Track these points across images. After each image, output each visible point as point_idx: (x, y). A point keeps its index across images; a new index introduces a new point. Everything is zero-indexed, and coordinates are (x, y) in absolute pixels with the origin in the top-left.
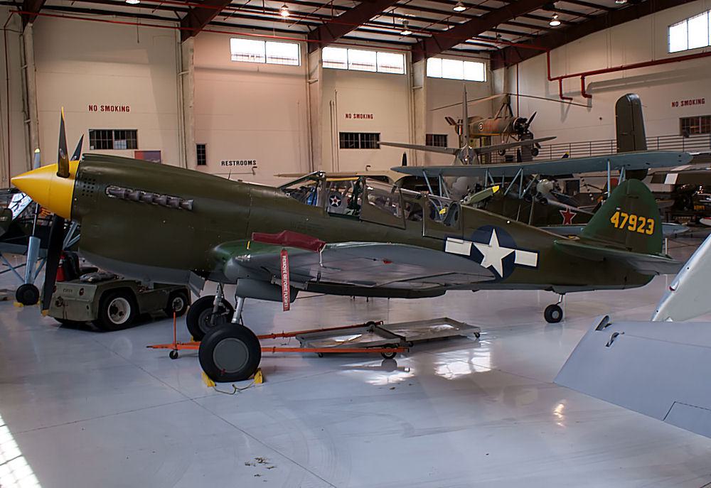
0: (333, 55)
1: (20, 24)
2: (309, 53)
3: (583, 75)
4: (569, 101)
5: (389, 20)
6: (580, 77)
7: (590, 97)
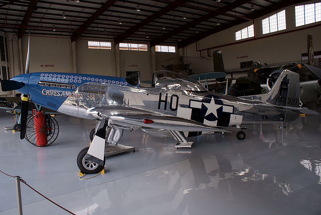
0: (123, 45)
1: (17, 39)
2: (115, 45)
3: (208, 49)
5: (141, 33)
6: (207, 50)
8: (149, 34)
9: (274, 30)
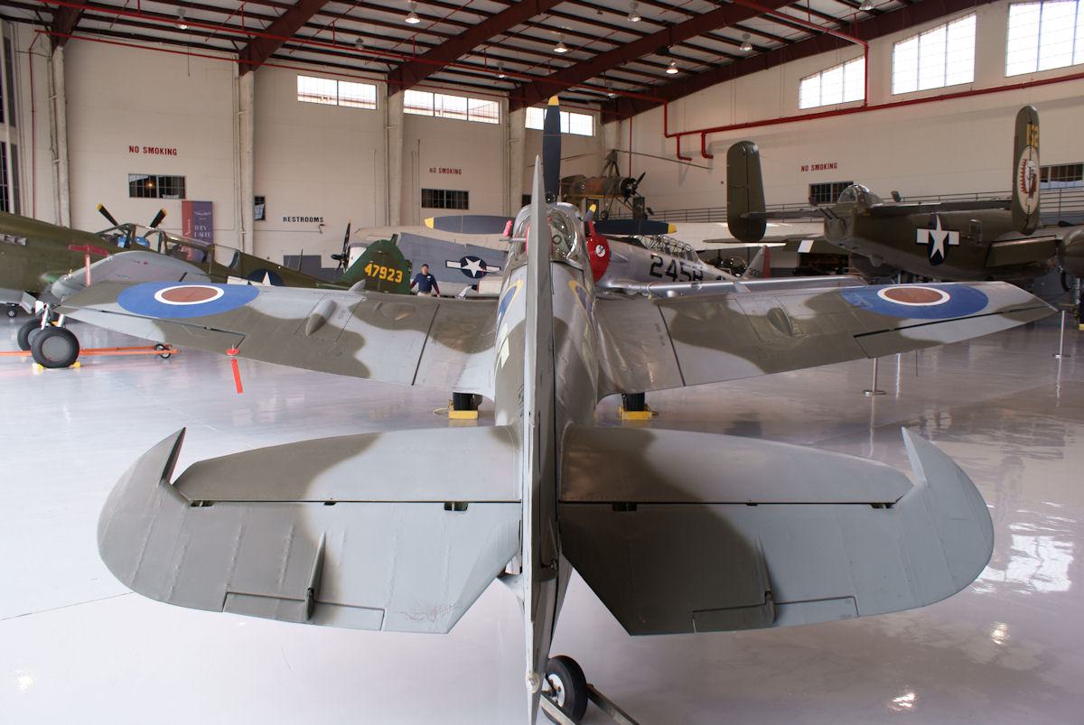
0: (417, 100)
3: (704, 133)
4: (687, 162)
5: (480, 60)
6: (700, 134)
7: (711, 157)
8: (508, 65)
9: (932, 81)
